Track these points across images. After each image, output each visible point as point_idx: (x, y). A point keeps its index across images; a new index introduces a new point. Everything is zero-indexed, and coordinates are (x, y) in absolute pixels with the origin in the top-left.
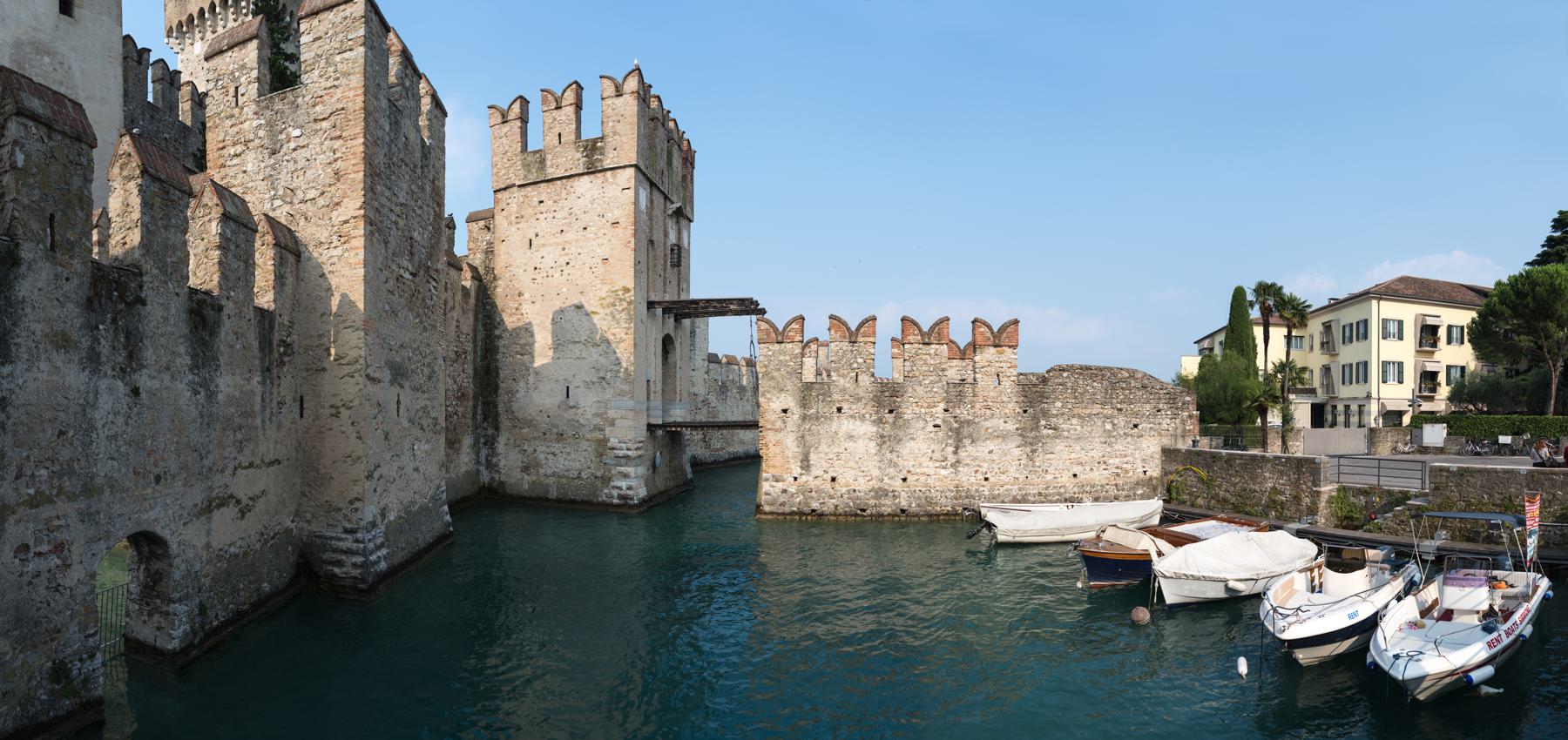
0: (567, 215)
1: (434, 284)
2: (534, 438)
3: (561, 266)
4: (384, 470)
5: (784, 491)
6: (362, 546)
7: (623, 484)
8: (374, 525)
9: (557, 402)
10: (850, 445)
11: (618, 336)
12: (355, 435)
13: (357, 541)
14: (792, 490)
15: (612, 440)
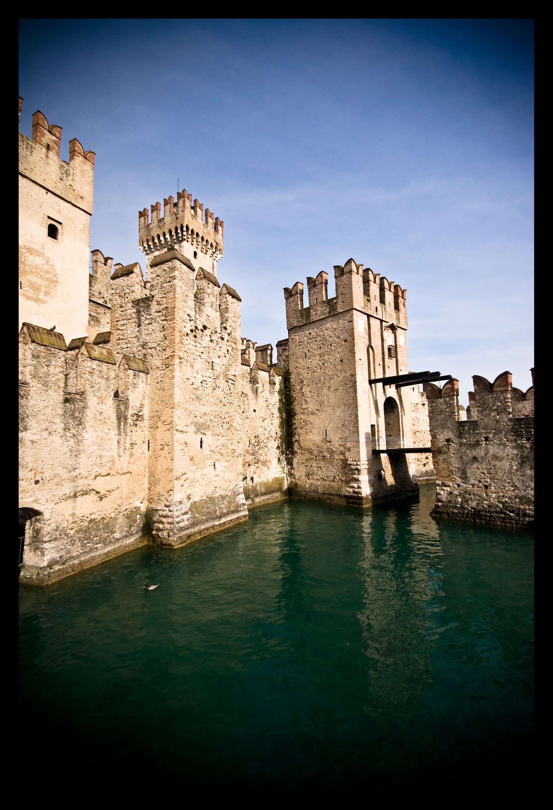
0: (322, 339)
1: (233, 382)
2: (311, 459)
3: (320, 366)
4: (190, 475)
5: (451, 493)
6: (172, 513)
7: (356, 485)
8: (181, 503)
9: (321, 439)
10: (497, 463)
11: (350, 401)
12: (170, 459)
13: (170, 511)
14: (456, 492)
15: (349, 459)
